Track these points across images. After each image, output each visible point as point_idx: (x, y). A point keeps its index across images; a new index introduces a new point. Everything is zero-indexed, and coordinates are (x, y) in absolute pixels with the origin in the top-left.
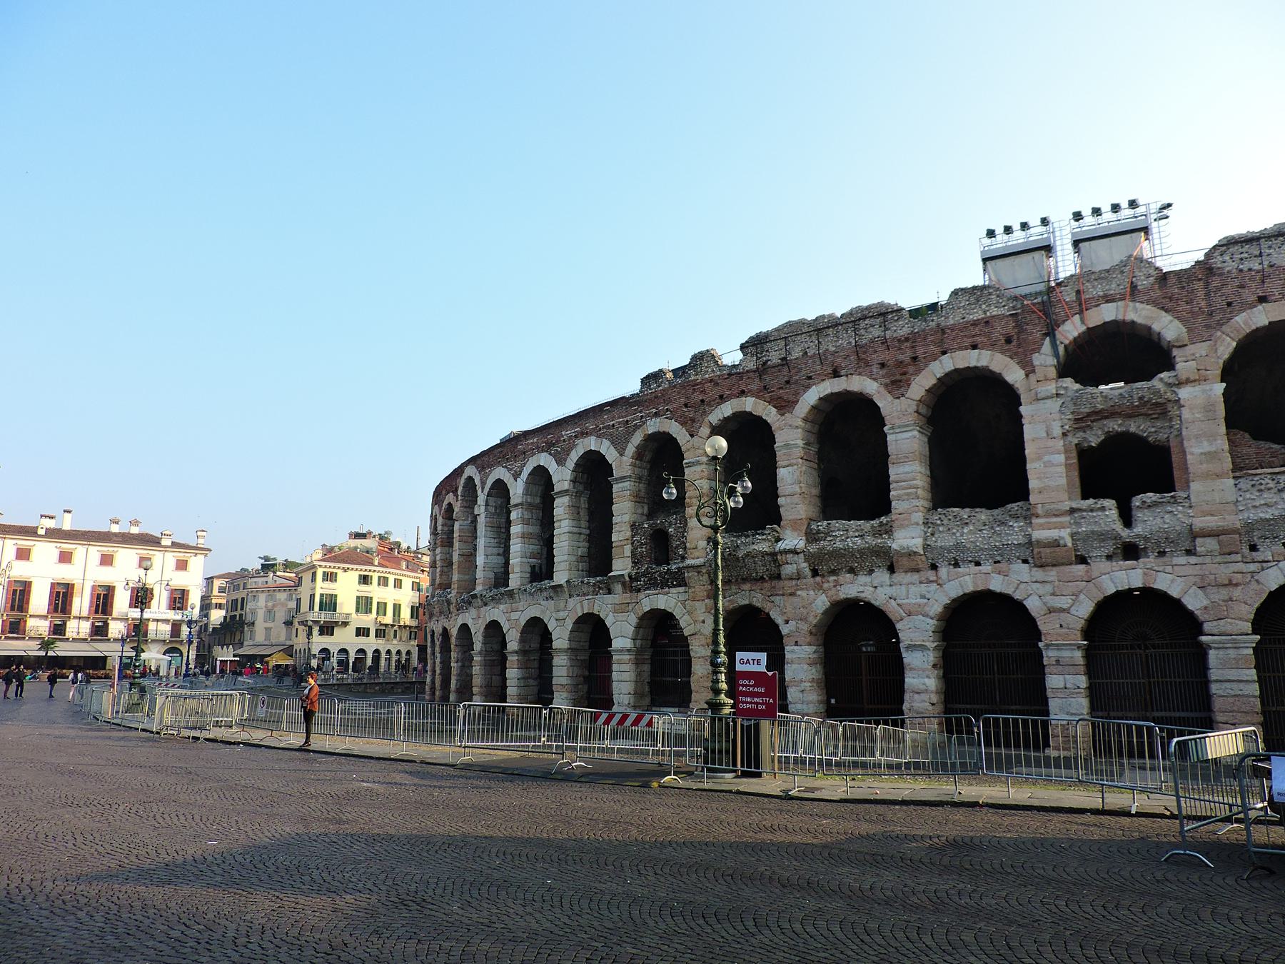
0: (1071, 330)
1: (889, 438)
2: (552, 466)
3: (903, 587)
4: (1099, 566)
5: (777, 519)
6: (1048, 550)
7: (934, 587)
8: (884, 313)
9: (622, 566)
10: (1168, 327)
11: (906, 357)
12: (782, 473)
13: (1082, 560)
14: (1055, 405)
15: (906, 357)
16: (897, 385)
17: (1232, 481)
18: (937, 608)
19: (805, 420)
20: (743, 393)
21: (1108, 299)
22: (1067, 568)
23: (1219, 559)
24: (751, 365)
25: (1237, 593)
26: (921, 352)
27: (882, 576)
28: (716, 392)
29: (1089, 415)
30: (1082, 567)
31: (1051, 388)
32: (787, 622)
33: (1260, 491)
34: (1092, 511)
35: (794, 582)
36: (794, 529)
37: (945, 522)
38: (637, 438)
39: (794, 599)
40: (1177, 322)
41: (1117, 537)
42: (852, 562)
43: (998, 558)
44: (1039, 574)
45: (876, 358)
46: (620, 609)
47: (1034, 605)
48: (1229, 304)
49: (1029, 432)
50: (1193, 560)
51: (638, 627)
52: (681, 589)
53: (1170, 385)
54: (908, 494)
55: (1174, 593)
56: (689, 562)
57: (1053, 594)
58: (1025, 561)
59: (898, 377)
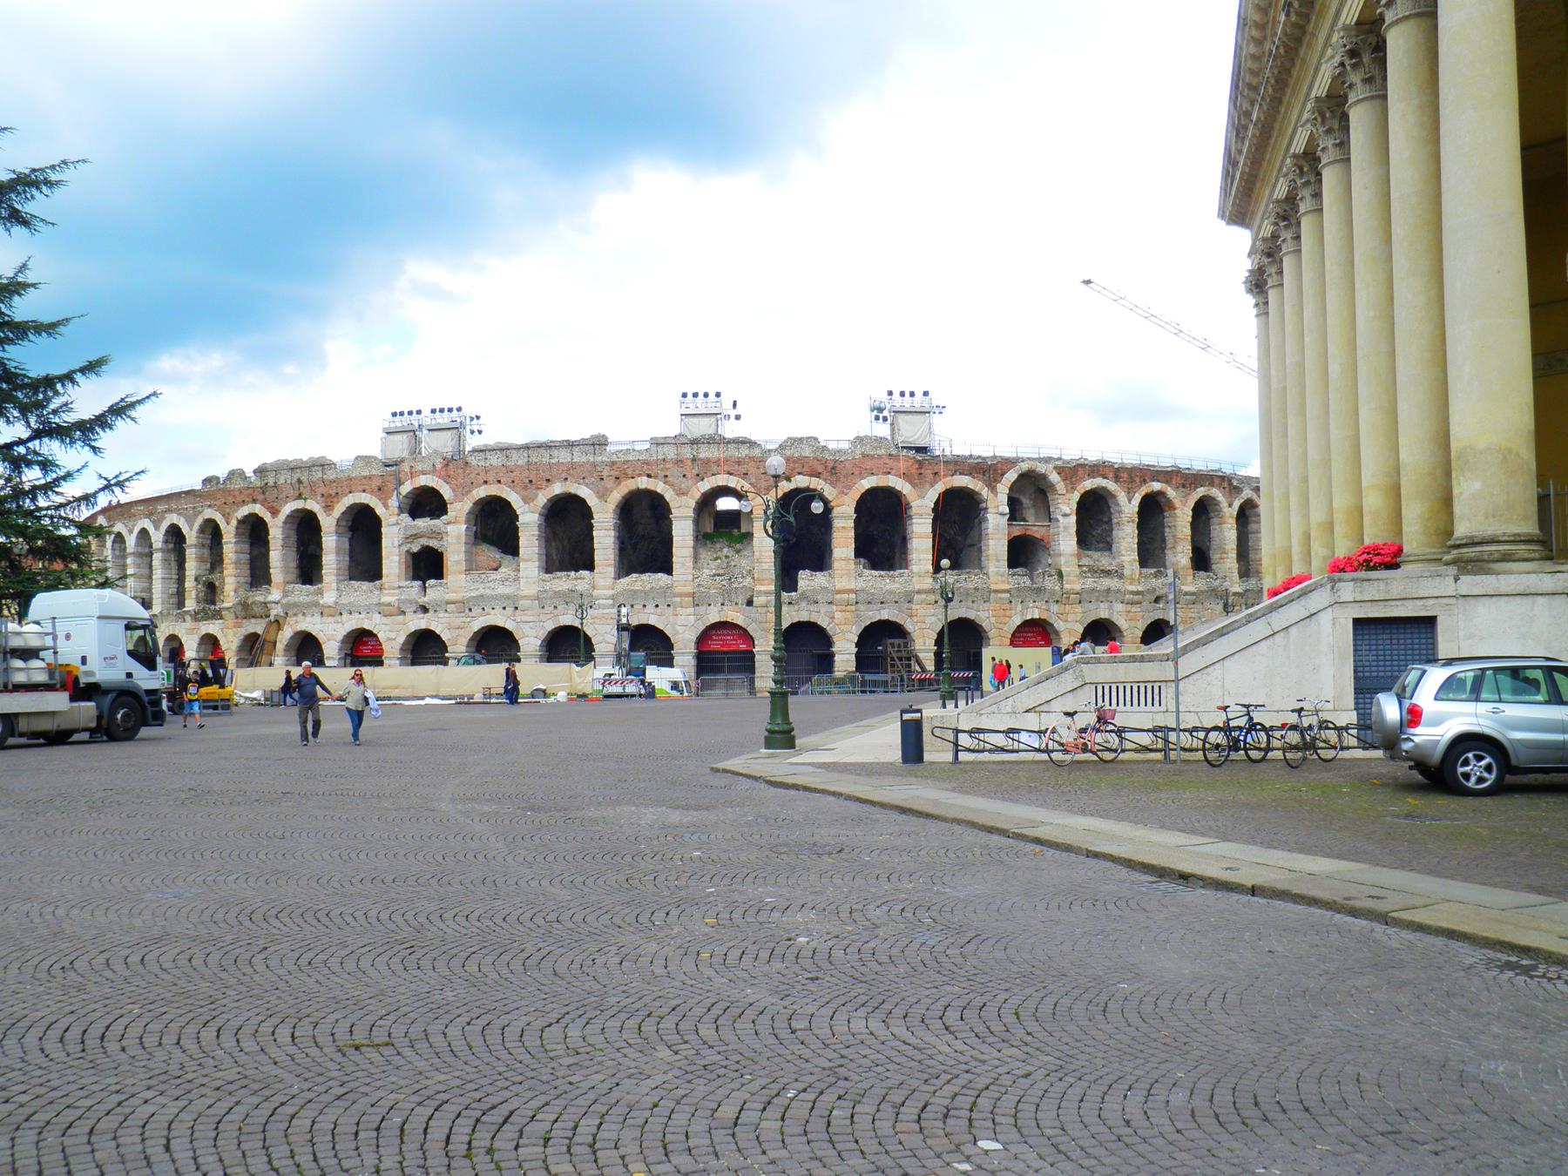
0: (406, 488)
2: (151, 530)
4: (410, 616)
5: (269, 582)
8: (323, 465)
9: (190, 604)
10: (446, 492)
13: (404, 613)
14: (396, 529)
16: (328, 508)
18: (340, 637)
19: (285, 523)
20: (254, 501)
24: (259, 484)
27: (317, 618)
28: (239, 499)
31: (394, 519)
42: (303, 609)
44: (385, 620)
45: (321, 490)
46: (190, 631)
47: (381, 636)
51: (200, 644)
56: (226, 605)
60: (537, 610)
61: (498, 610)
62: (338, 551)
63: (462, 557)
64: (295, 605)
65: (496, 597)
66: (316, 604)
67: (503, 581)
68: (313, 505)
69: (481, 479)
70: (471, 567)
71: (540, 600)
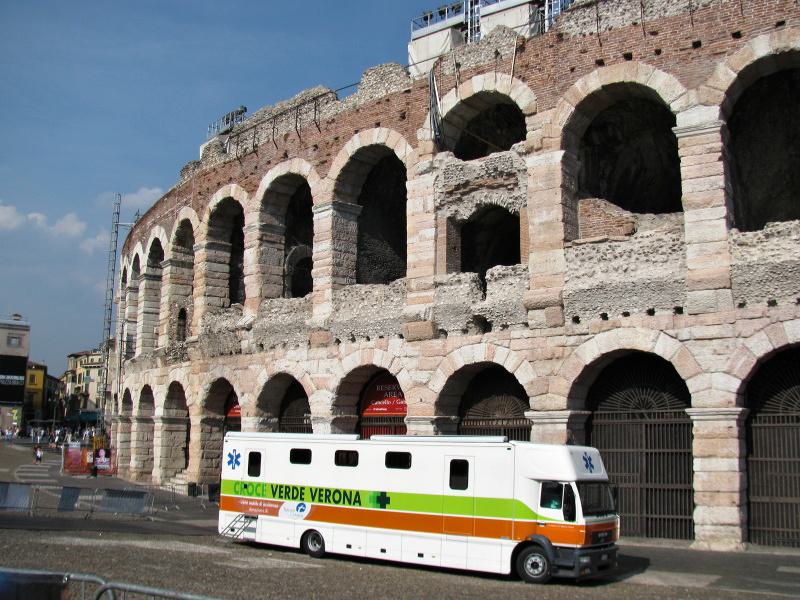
0: (448, 103)
1: (315, 217)
3: (316, 362)
6: (413, 324)
7: (336, 360)
10: (522, 96)
11: (330, 138)
12: (247, 253)
14: (429, 178)
15: (330, 138)
16: (323, 165)
17: (562, 251)
18: (335, 383)
21: (480, 71)
22: (427, 342)
23: (547, 332)
25: (557, 366)
26: (341, 132)
27: (303, 351)
29: (458, 187)
30: (438, 343)
31: (425, 163)
32: (243, 394)
33: (583, 261)
34: (451, 285)
35: (249, 356)
36: (252, 307)
37: (349, 297)
38: (176, 225)
39: (247, 372)
40: (529, 89)
41: (468, 311)
43: (382, 333)
44: (410, 349)
45: (311, 141)
47: (403, 380)
48: (572, 70)
49: (412, 206)
50: (527, 332)
52: (188, 363)
53: (520, 154)
54: (323, 272)
55: (509, 368)
57: (417, 369)
58: (401, 336)
59: (325, 158)
60: (728, 309)
61: (638, 316)
62: (336, 237)
63: (557, 213)
64: (271, 330)
65: (633, 289)
66: (300, 327)
67: (647, 254)
68: (301, 166)
69: (589, 59)
70: (571, 231)
71: (737, 287)
